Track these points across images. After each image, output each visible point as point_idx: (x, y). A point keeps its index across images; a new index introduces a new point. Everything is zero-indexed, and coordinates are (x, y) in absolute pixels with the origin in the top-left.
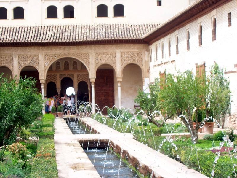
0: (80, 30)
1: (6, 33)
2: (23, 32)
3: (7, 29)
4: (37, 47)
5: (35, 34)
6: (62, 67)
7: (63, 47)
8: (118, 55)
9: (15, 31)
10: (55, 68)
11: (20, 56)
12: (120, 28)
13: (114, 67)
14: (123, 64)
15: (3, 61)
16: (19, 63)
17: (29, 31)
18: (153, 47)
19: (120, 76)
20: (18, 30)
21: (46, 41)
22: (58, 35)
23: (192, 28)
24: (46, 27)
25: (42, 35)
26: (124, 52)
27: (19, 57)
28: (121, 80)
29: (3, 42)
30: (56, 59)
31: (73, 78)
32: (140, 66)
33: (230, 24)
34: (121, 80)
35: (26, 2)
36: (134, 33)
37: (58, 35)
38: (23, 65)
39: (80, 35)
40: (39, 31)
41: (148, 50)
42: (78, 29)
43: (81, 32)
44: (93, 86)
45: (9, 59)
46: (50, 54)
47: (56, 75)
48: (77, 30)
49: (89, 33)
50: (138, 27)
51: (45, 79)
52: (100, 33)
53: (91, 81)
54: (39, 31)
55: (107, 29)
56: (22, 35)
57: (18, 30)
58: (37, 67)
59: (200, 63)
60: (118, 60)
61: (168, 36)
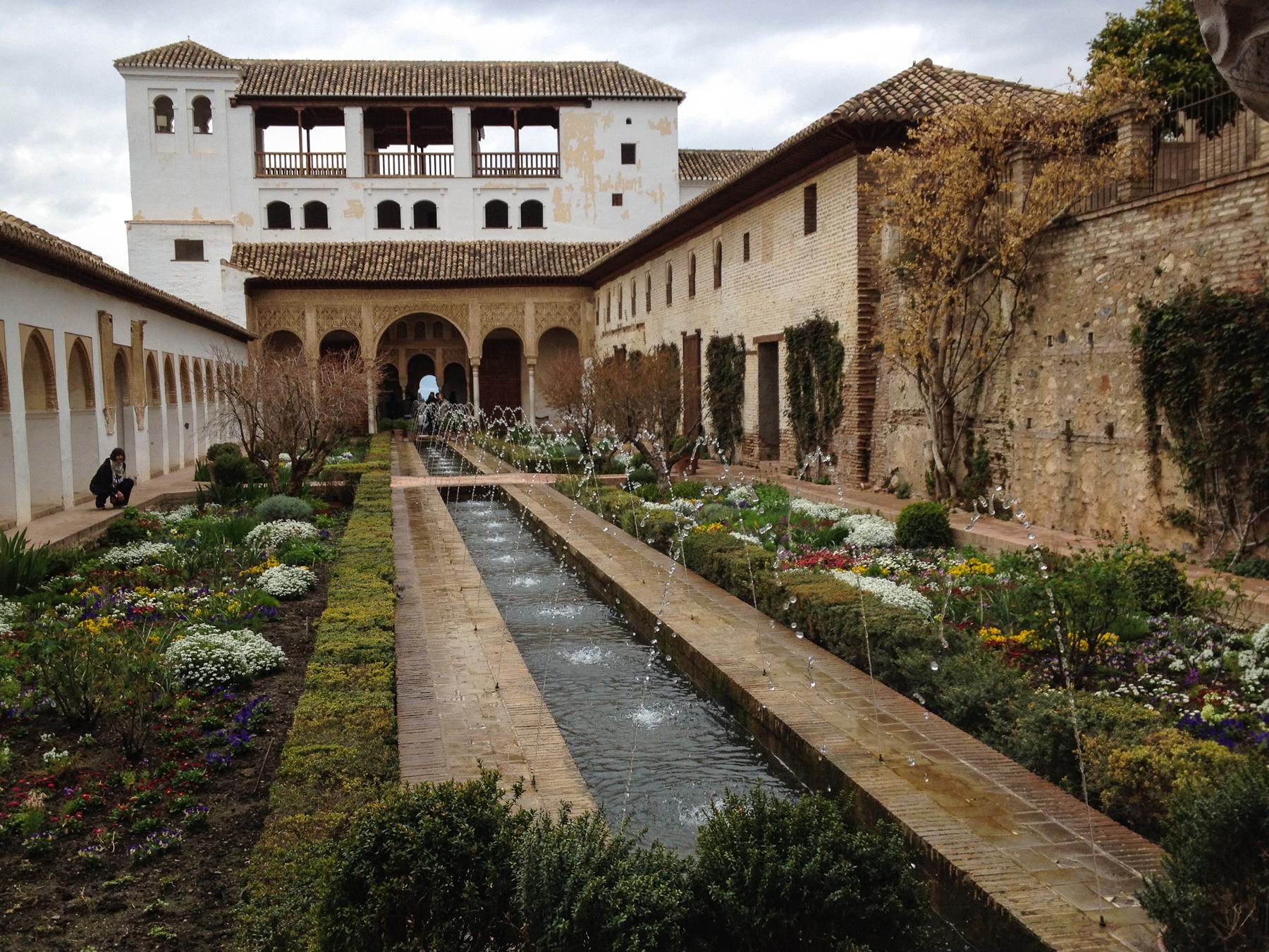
6: (411, 337)
8: (530, 309)
11: (321, 310)
18: (601, 294)
21: (375, 278)
22: (402, 265)
23: (677, 258)
25: (367, 264)
30: (397, 316)
33: (747, 257)
37: (402, 265)
38: (327, 329)
41: (592, 300)
43: (451, 259)
44: (475, 373)
45: (296, 316)
58: (357, 334)
59: (691, 333)
60: (529, 317)
61: (632, 274)
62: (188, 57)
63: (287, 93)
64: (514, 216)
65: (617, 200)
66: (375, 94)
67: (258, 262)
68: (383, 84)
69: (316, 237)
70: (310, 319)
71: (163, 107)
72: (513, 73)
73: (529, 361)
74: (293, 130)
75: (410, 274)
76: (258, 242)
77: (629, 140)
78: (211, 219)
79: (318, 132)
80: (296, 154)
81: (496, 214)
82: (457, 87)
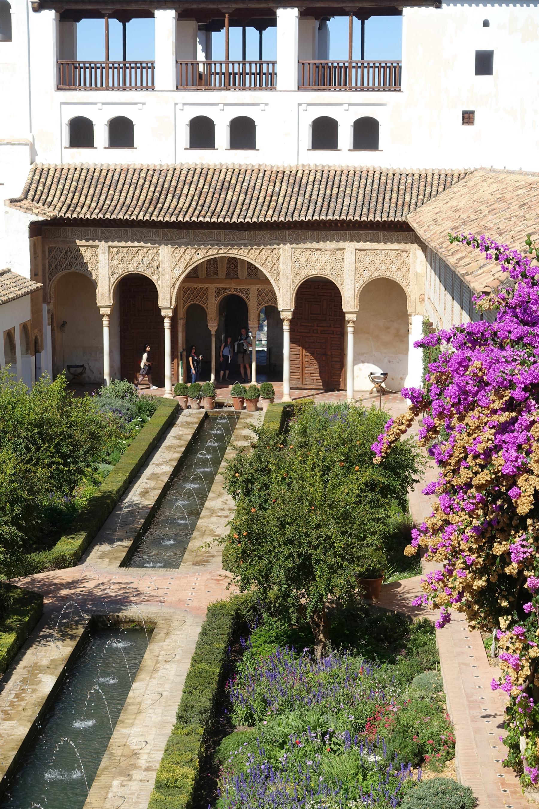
0: (265, 183)
1: (86, 186)
2: (126, 186)
3: (90, 173)
5: (154, 192)
6: (222, 272)
9: (108, 182)
10: (205, 271)
12: (363, 181)
14: (362, 280)
15: (74, 260)
19: (352, 309)
20: (116, 178)
21: (173, 219)
24: (184, 172)
28: (354, 317)
29: (73, 216)
31: (248, 297)
32: (403, 284)
34: (355, 319)
35: (140, 106)
36: (394, 200)
39: (261, 200)
40: (166, 186)
42: (259, 181)
44: (286, 327)
47: (207, 288)
48: (258, 185)
50: (410, 180)
51: (172, 307)
52: (311, 196)
53: (282, 317)
54: (166, 186)
55: (330, 183)
56: (124, 194)
58: (154, 278)
60: (348, 266)
64: (345, 135)
65: (468, 118)
73: (348, 317)
76: (58, 163)
77: (485, 47)
78: (7, 138)
81: (324, 133)
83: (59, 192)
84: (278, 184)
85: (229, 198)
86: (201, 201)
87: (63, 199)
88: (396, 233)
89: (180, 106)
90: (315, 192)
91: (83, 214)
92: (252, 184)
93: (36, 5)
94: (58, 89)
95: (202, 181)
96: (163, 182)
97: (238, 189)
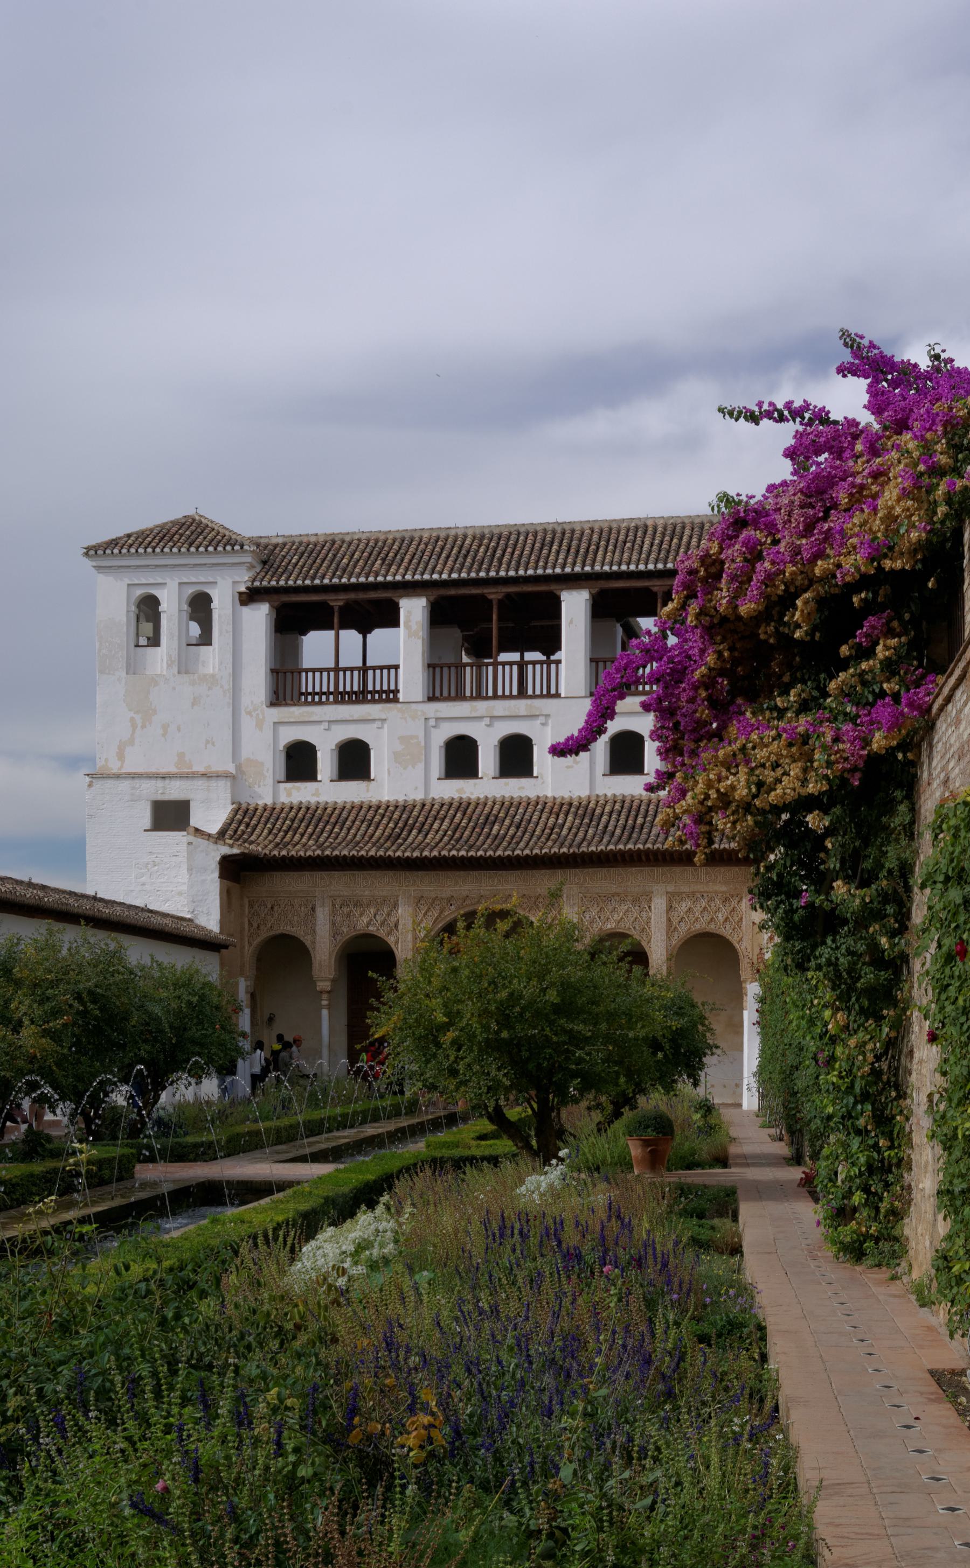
0: (544, 816)
4: (391, 873)
7: (476, 873)
8: (659, 904)
9: (332, 820)
11: (339, 901)
13: (644, 944)
16: (334, 924)
17: (378, 818)
20: (344, 815)
22: (467, 833)
25: (414, 832)
26: (679, 894)
27: (334, 905)
35: (378, 724)
37: (467, 833)
38: (347, 932)
40: (411, 822)
46: (433, 895)
48: (535, 818)
49: (570, 829)
52: (606, 827)
55: (633, 813)
57: (344, 815)
58: (391, 940)
62: (190, 536)
63: (317, 582)
66: (445, 576)
67: (258, 831)
68: (460, 559)
69: (352, 792)
70: (323, 916)
71: (148, 608)
72: (664, 534)
74: (327, 636)
75: (471, 847)
78: (202, 769)
79: (378, 636)
80: (328, 670)
82: (570, 560)
83: (266, 831)
84: (562, 816)
85: (494, 832)
86: (457, 835)
87: (270, 838)
88: (723, 869)
89: (432, 722)
90: (612, 823)
91: (296, 851)
92: (527, 817)
93: (244, 596)
94: (272, 704)
95: (459, 815)
96: (406, 817)
97: (507, 822)
